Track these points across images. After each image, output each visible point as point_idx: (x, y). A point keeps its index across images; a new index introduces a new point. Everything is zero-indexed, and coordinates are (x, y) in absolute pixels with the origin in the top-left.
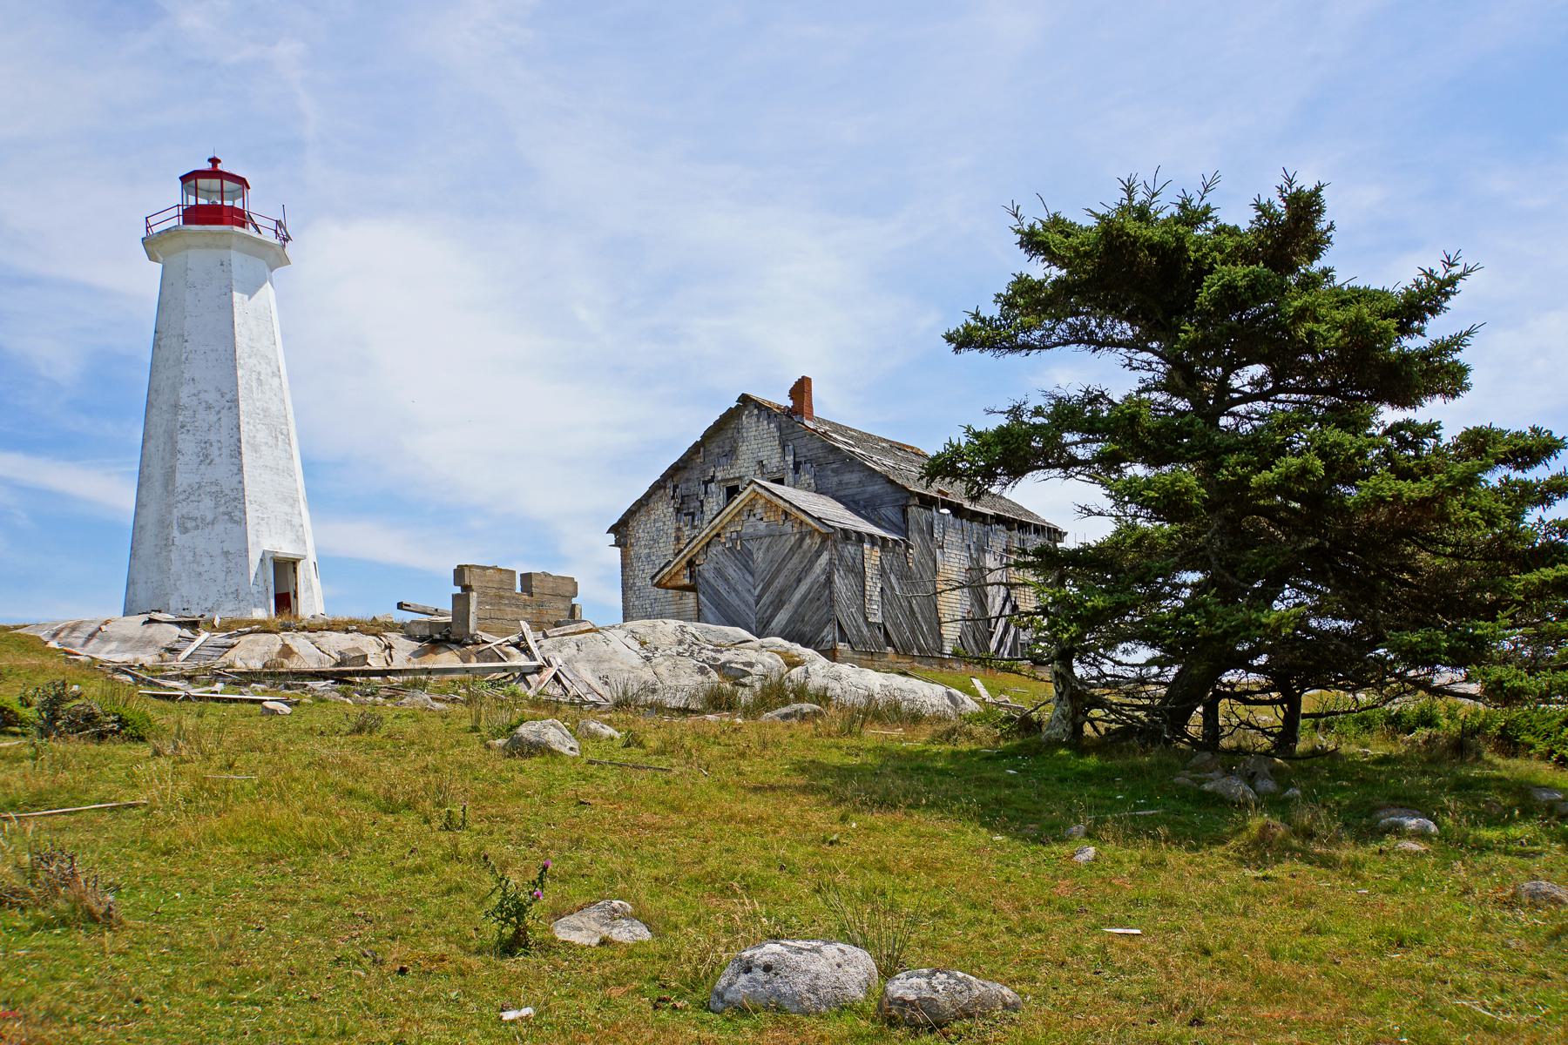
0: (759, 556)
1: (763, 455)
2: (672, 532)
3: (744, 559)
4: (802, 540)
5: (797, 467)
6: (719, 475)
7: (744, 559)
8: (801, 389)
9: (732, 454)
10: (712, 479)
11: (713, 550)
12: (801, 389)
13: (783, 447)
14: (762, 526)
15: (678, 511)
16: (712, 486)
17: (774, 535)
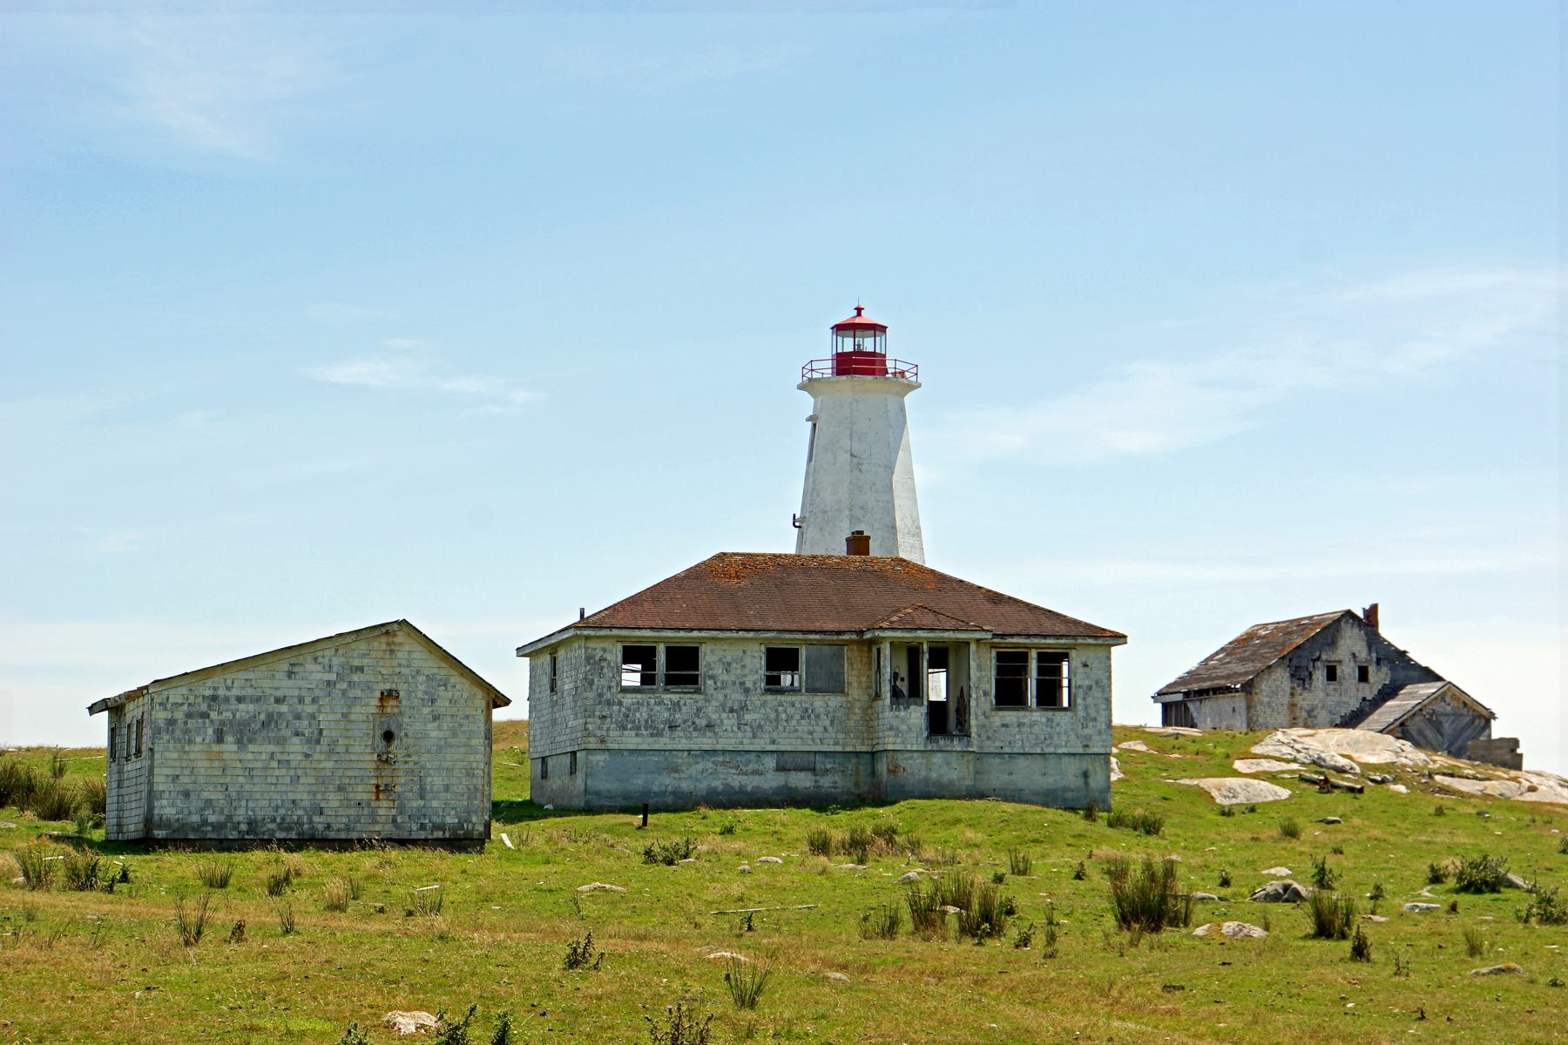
0: (1446, 725)
1: (1356, 650)
2: (1288, 689)
3: (1437, 727)
4: (1473, 721)
5: (1378, 662)
6: (1324, 657)
7: (1437, 727)
8: (1372, 612)
9: (1333, 644)
10: (1318, 659)
11: (1417, 719)
12: (1372, 612)
13: (1370, 648)
14: (1449, 708)
15: (1292, 676)
16: (1319, 664)
17: (1457, 715)
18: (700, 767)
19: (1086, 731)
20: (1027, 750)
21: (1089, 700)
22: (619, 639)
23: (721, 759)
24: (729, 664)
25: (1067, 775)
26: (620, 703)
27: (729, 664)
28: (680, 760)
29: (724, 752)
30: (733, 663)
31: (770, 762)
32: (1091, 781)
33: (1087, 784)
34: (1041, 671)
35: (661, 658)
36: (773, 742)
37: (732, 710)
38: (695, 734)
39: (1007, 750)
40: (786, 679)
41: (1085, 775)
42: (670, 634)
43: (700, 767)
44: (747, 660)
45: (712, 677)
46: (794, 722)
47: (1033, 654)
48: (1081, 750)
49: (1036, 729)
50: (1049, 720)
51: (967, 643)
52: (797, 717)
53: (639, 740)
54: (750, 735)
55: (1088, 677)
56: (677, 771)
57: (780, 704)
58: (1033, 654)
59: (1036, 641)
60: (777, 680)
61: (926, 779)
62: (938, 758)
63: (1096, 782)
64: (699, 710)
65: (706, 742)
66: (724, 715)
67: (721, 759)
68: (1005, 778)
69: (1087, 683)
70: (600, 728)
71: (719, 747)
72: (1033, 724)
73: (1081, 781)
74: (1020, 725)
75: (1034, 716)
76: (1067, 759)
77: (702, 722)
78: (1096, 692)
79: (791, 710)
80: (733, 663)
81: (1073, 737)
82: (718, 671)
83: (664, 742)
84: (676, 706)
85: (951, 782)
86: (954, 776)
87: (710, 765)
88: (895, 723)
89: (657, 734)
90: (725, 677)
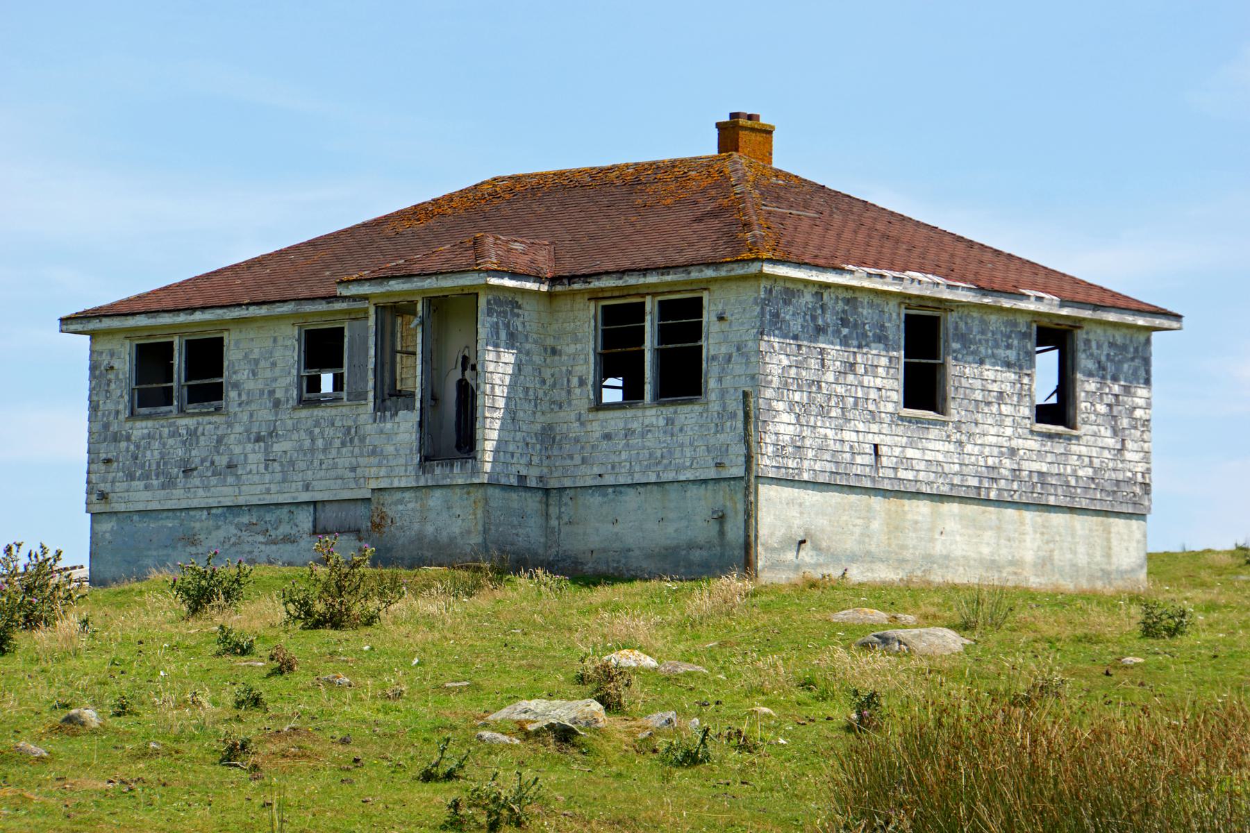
18: (221, 534)
19: (722, 437)
20: (638, 478)
21: (728, 382)
22: (129, 333)
23: (245, 519)
24: (257, 362)
25: (687, 519)
26: (128, 438)
27: (257, 362)
28: (199, 523)
29: (250, 507)
30: (262, 359)
31: (305, 520)
32: (729, 527)
33: (722, 533)
34: (665, 334)
35: (178, 361)
36: (307, 488)
37: (259, 439)
38: (214, 480)
39: (609, 480)
40: (327, 382)
41: (721, 519)
42: (142, 321)
43: (221, 534)
44: (278, 354)
45: (236, 386)
46: (334, 452)
47: (650, 305)
48: (712, 473)
49: (650, 440)
50: (670, 422)
51: (471, 296)
52: (337, 443)
53: (148, 495)
54: (278, 476)
55: (726, 340)
56: (193, 544)
57: (317, 424)
58: (650, 305)
59: (652, 279)
60: (314, 384)
61: (420, 537)
62: (435, 499)
63: (734, 531)
64: (220, 440)
65: (225, 494)
66: (249, 446)
67: (245, 519)
68: (607, 529)
69: (723, 350)
70: (104, 481)
71: (241, 501)
72: (647, 430)
73: (714, 528)
74: (629, 433)
75: (651, 415)
76: (693, 491)
77: (222, 461)
78: (737, 367)
79: (329, 432)
80: (262, 359)
81: (702, 451)
82: (243, 375)
83: (177, 498)
84: (193, 433)
85: (452, 539)
86: (456, 528)
87: (233, 530)
88: (378, 441)
89: (169, 484)
90: (250, 385)
